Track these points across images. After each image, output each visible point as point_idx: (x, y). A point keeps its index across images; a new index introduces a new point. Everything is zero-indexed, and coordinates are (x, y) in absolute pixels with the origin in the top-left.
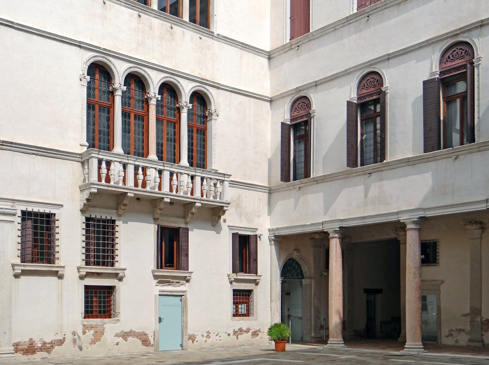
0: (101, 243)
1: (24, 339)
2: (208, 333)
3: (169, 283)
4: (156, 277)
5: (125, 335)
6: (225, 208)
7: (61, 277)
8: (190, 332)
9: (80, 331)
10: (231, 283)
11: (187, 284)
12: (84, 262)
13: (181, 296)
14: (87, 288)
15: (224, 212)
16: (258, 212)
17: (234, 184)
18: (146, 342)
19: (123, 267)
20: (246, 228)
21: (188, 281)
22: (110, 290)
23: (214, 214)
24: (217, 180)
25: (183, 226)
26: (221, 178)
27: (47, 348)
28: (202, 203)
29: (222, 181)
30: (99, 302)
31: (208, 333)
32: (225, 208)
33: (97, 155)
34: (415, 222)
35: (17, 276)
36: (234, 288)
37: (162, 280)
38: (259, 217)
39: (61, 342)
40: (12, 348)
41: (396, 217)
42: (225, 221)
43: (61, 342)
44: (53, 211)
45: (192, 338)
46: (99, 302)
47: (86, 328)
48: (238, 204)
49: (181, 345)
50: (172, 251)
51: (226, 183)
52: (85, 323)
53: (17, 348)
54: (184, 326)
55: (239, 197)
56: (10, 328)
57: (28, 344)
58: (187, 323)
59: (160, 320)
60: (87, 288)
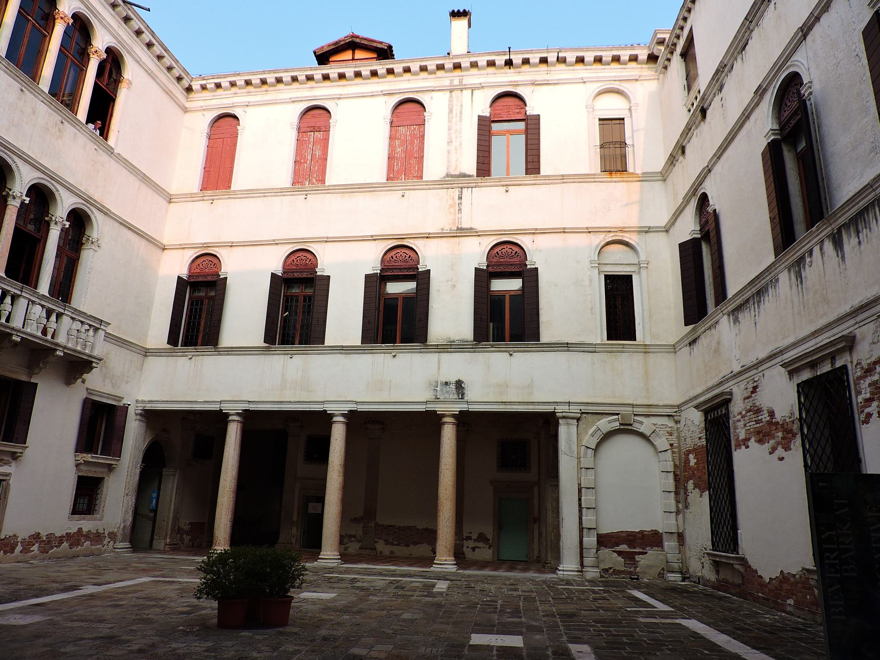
6: (94, 365)
10: (77, 466)
11: (13, 464)
15: (92, 368)
17: (108, 336)
20: (109, 396)
24: (90, 326)
25: (24, 378)
26: (96, 324)
28: (64, 353)
29: (96, 330)
32: (94, 365)
34: (343, 415)
38: (127, 383)
41: (321, 406)
42: (83, 381)
51: (101, 333)
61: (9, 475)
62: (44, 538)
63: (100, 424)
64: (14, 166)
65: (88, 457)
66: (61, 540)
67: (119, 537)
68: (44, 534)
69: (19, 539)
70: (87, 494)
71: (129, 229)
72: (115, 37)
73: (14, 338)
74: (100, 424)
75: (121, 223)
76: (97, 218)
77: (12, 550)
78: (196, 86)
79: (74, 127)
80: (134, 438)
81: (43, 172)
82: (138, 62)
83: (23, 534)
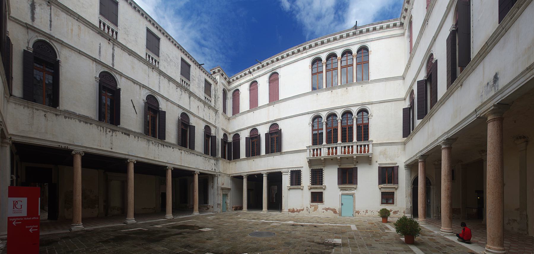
0: (317, 177)
1: (291, 208)
2: (367, 211)
3: (346, 190)
4: (339, 188)
5: (327, 209)
7: (302, 189)
8: (357, 210)
13: (353, 195)
14: (312, 193)
18: (335, 212)
20: (392, 164)
21: (355, 189)
23: (368, 160)
25: (353, 166)
27: (298, 211)
30: (317, 198)
31: (367, 211)
33: (315, 147)
35: (289, 190)
37: (342, 189)
39: (303, 210)
43: (303, 210)
45: (358, 212)
46: (317, 198)
47: (311, 206)
50: (348, 177)
53: (289, 210)
59: (342, 204)
60: (312, 193)
63: (388, 175)
65: (382, 186)
70: (388, 198)
74: (388, 175)
80: (403, 176)
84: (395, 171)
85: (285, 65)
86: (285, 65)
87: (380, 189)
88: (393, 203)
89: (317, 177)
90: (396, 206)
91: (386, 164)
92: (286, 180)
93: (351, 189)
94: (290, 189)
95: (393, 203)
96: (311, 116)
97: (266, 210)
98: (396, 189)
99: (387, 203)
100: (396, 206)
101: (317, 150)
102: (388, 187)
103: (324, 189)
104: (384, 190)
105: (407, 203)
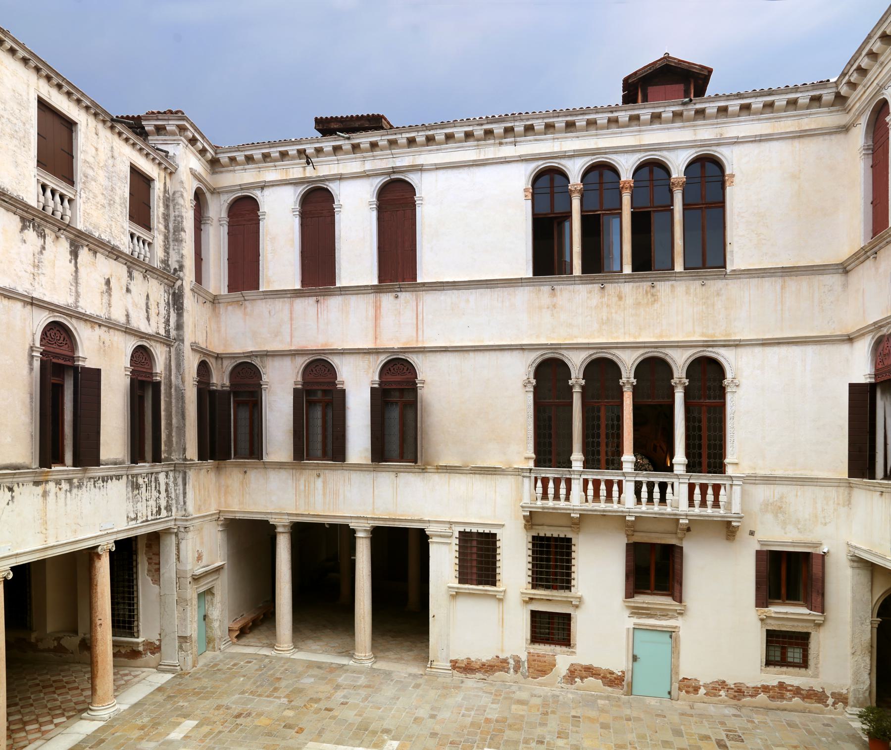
4: (628, 607)
9: (524, 657)
11: (680, 618)
12: (530, 586)
13: (672, 633)
16: (824, 517)
19: (579, 594)
22: (567, 617)
30: (551, 629)
36: (769, 628)
37: (637, 612)
40: (449, 664)
44: (493, 531)
46: (551, 629)
48: (780, 508)
49: (669, 693)
52: (532, 651)
53: (455, 665)
54: (674, 669)
55: (781, 498)
56: (448, 646)
57: (465, 663)
58: (678, 666)
59: (635, 658)
60: (534, 614)
61: (675, 627)
62: (732, 686)
63: (788, 575)
64: (615, 359)
66: (755, 692)
67: (851, 700)
68: (731, 682)
69: (701, 683)
70: (786, 647)
71: (779, 343)
72: (692, 147)
73: (628, 518)
74: (788, 575)
75: (763, 345)
76: (725, 356)
77: (696, 689)
78: (844, 90)
79: (668, 280)
81: (645, 347)
82: (737, 142)
83: (705, 677)
84: (816, 569)
85: (438, 167)
86: (438, 167)
87: (762, 620)
88: (804, 664)
89: (552, 561)
90: (816, 676)
91: (793, 544)
92: (443, 563)
93: (665, 614)
94: (456, 595)
95: (804, 664)
96: (532, 359)
97: (369, 654)
98: (819, 625)
99: (783, 662)
100: (816, 676)
101: (557, 482)
102: (790, 614)
103: (577, 607)
104: (775, 626)
105: (856, 674)
